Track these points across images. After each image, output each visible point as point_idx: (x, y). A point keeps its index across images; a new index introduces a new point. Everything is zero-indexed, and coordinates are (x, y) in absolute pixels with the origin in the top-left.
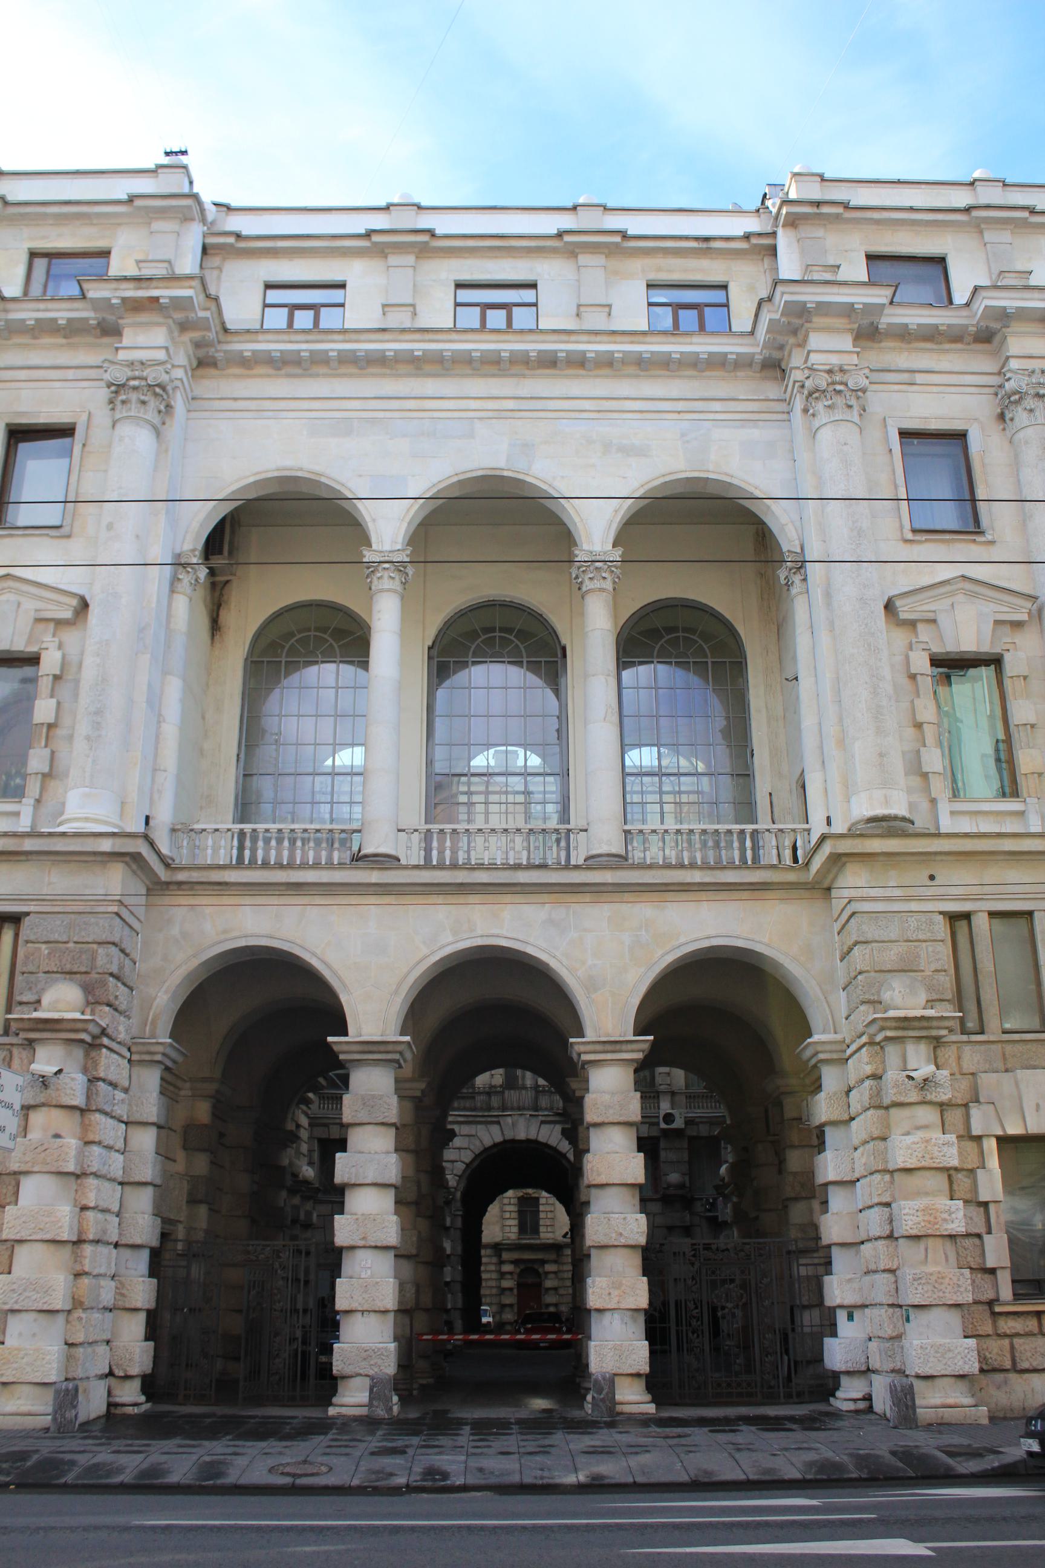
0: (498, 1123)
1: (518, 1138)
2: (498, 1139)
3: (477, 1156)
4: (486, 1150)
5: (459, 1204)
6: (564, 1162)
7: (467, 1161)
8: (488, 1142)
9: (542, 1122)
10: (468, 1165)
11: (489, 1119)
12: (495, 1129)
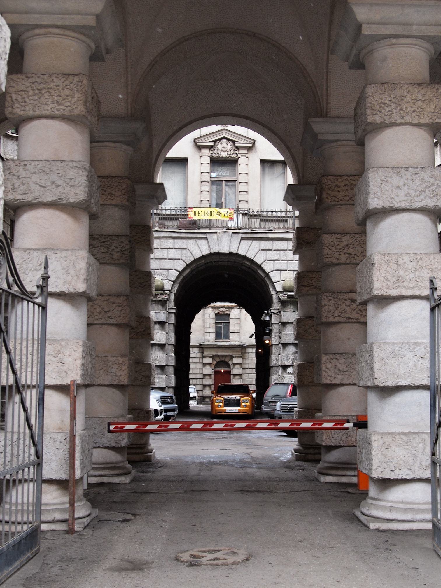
0: (206, 238)
1: (222, 251)
2: (206, 252)
3: (188, 266)
4: (195, 261)
5: (172, 304)
6: (260, 272)
7: (180, 269)
8: (197, 255)
9: (242, 239)
10: (181, 273)
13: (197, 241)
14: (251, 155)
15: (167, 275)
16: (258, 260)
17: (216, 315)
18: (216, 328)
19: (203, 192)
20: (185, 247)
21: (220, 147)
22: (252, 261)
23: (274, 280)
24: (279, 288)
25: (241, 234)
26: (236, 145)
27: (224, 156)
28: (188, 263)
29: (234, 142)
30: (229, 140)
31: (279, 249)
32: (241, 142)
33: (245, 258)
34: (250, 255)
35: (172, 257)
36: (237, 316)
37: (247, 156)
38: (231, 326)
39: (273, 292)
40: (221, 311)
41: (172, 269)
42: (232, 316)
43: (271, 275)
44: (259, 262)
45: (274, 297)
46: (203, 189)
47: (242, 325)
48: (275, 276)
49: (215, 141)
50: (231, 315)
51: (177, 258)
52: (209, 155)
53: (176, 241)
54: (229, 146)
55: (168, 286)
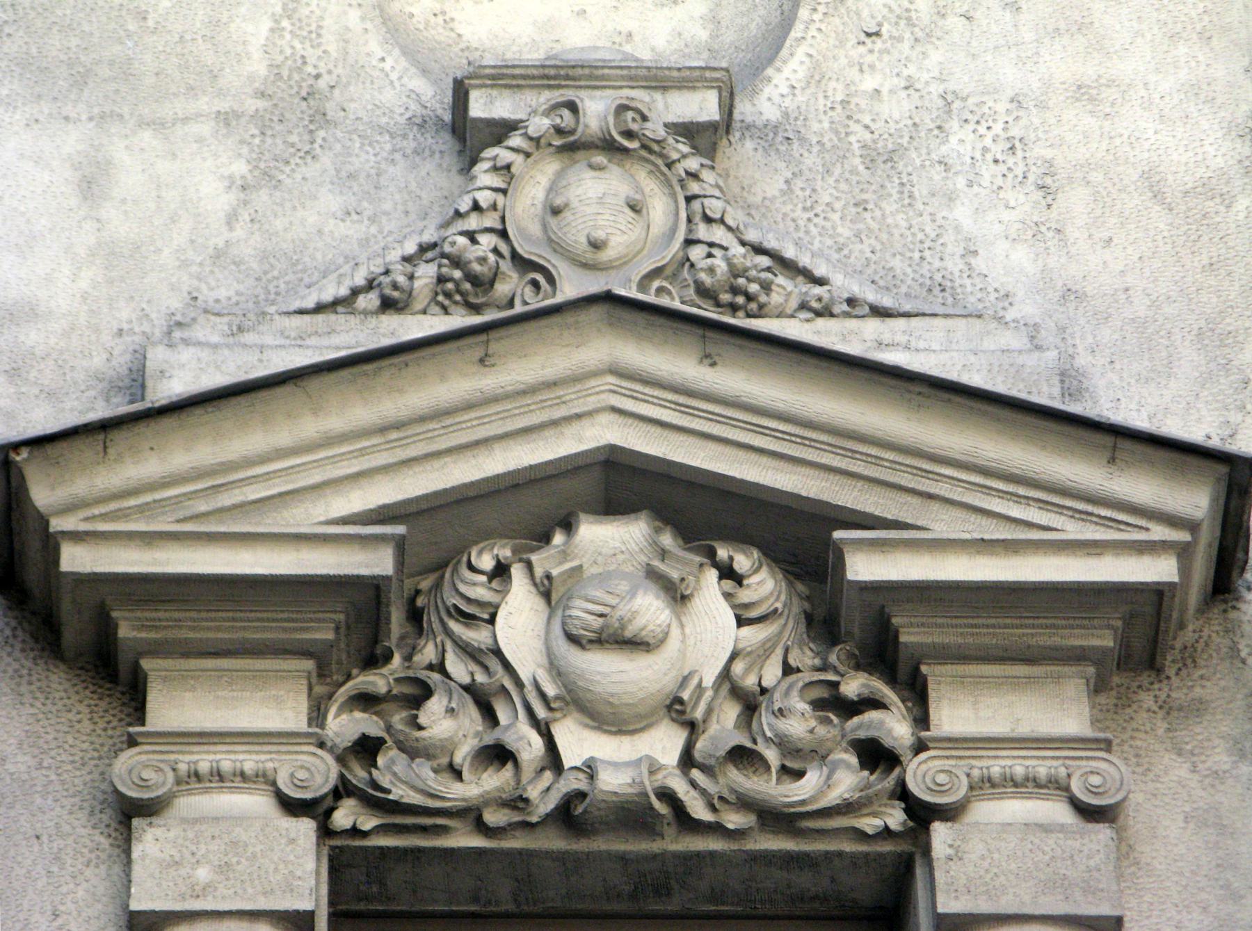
21: (520, 625)
26: (864, 567)
27: (613, 782)
29: (800, 540)
30: (699, 513)
32: (943, 524)
37: (1094, 776)
49: (437, 532)
52: (315, 772)
54: (712, 628)
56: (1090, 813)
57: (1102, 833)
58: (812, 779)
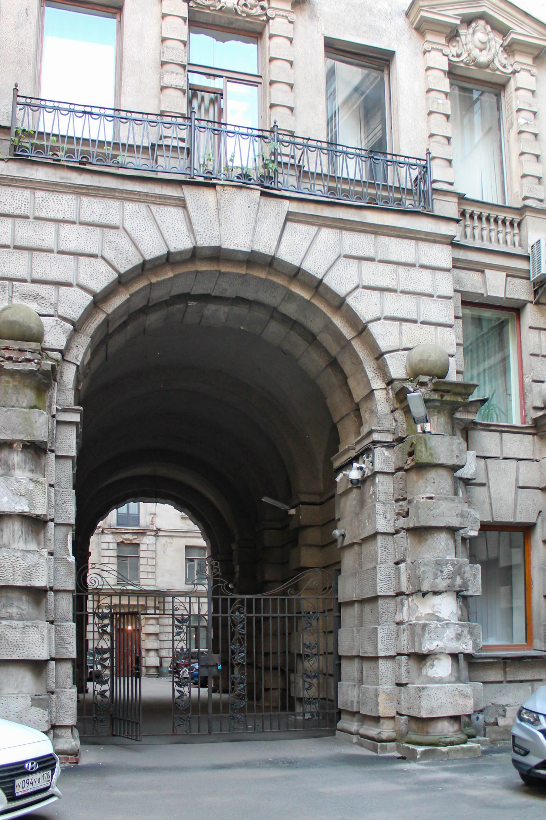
0: (182, 204)
1: (229, 244)
2: (181, 242)
3: (122, 281)
6: (338, 322)
7: (98, 286)
8: (153, 249)
9: (290, 217)
10: (99, 300)
11: (158, 190)
12: (171, 216)
13: (154, 208)
14: (301, 18)
15: (53, 300)
16: (340, 281)
17: (118, 544)
18: (119, 565)
19: (167, 91)
20: (116, 221)
22: (317, 286)
23: (383, 344)
24: (397, 368)
25: (287, 202)
28: (122, 271)
31: (394, 258)
33: (297, 274)
34: (314, 266)
35: (72, 246)
36: (152, 548)
37: (292, 17)
38: (142, 561)
39: (377, 384)
40: (126, 540)
41: (69, 285)
42: (142, 547)
43: (375, 329)
44: (341, 290)
45: (380, 396)
46: (168, 80)
47: (160, 561)
48: (385, 336)
50: (141, 545)
51: (88, 251)
53: (85, 199)
55: (55, 336)
56: (291, 22)
57: (292, 25)
58: (255, 10)
